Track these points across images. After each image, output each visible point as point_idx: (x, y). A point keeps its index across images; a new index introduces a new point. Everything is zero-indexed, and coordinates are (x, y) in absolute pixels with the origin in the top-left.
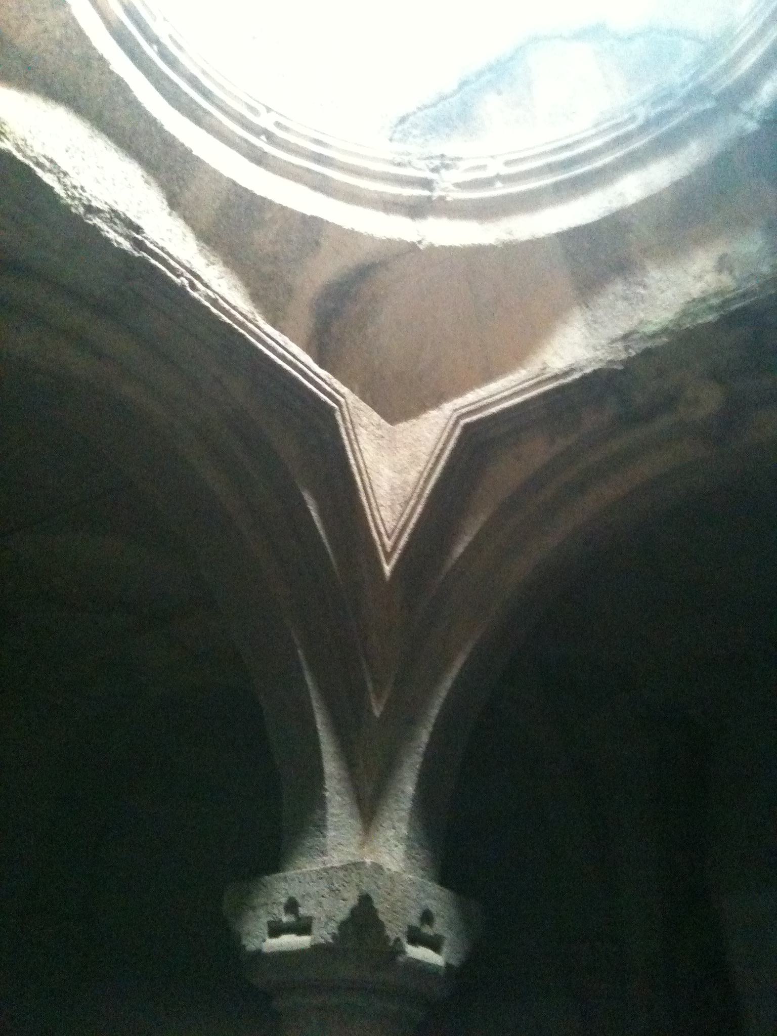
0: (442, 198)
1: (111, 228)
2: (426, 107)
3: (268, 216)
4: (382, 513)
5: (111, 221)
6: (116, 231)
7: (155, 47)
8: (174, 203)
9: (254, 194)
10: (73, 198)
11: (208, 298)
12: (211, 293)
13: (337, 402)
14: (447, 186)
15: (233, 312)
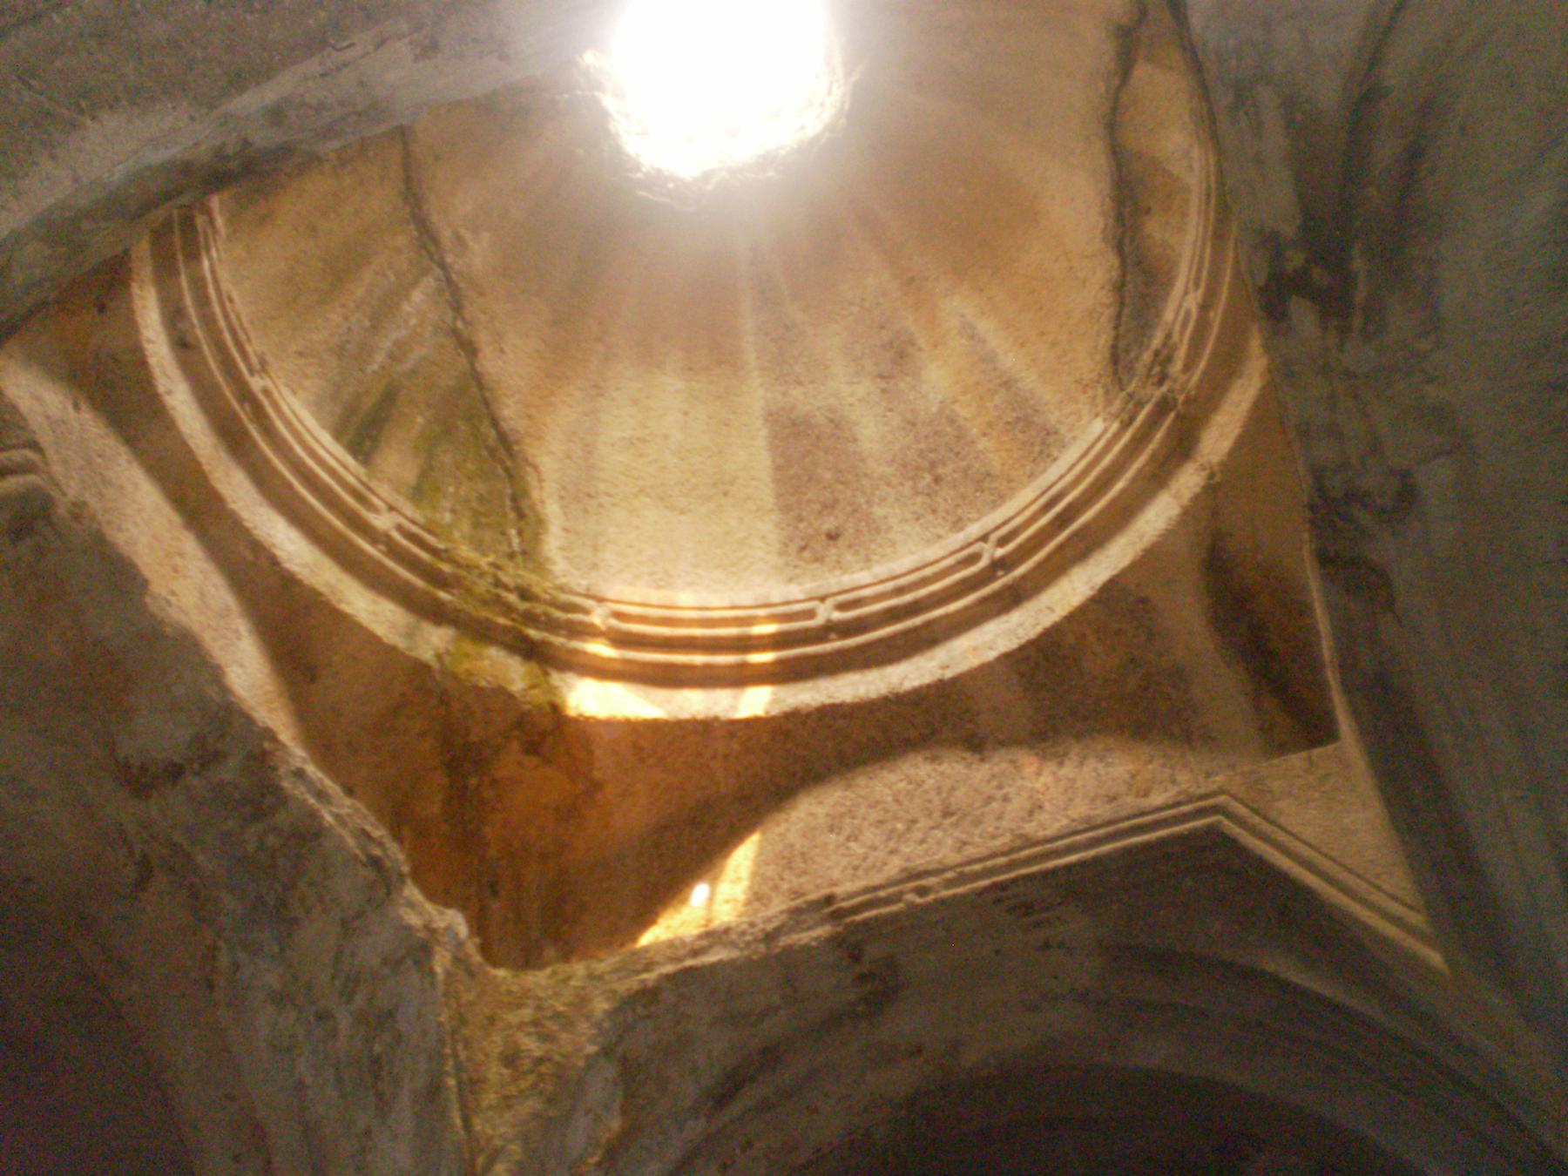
0: (1188, 400)
1: (803, 930)
2: (1119, 316)
3: (1071, 639)
4: (1386, 887)
5: (798, 922)
6: (809, 928)
7: (833, 636)
8: (976, 745)
9: (1032, 643)
10: (748, 944)
11: (950, 883)
12: (949, 875)
13: (1215, 810)
14: (1185, 379)
15: (989, 863)
